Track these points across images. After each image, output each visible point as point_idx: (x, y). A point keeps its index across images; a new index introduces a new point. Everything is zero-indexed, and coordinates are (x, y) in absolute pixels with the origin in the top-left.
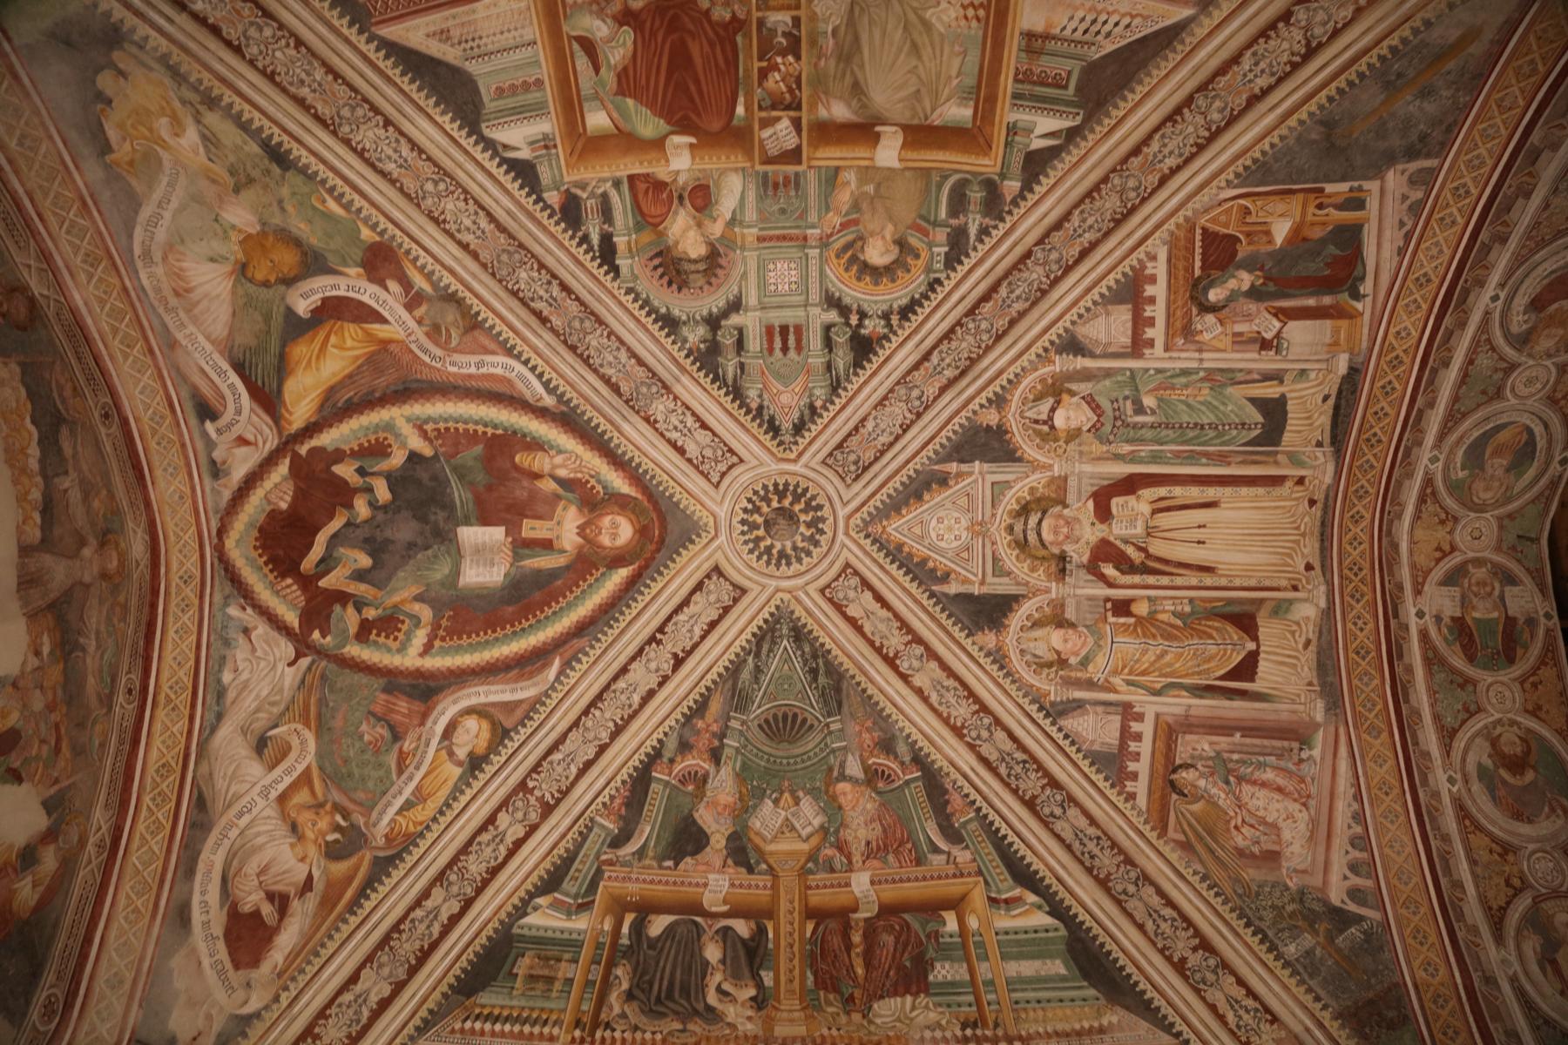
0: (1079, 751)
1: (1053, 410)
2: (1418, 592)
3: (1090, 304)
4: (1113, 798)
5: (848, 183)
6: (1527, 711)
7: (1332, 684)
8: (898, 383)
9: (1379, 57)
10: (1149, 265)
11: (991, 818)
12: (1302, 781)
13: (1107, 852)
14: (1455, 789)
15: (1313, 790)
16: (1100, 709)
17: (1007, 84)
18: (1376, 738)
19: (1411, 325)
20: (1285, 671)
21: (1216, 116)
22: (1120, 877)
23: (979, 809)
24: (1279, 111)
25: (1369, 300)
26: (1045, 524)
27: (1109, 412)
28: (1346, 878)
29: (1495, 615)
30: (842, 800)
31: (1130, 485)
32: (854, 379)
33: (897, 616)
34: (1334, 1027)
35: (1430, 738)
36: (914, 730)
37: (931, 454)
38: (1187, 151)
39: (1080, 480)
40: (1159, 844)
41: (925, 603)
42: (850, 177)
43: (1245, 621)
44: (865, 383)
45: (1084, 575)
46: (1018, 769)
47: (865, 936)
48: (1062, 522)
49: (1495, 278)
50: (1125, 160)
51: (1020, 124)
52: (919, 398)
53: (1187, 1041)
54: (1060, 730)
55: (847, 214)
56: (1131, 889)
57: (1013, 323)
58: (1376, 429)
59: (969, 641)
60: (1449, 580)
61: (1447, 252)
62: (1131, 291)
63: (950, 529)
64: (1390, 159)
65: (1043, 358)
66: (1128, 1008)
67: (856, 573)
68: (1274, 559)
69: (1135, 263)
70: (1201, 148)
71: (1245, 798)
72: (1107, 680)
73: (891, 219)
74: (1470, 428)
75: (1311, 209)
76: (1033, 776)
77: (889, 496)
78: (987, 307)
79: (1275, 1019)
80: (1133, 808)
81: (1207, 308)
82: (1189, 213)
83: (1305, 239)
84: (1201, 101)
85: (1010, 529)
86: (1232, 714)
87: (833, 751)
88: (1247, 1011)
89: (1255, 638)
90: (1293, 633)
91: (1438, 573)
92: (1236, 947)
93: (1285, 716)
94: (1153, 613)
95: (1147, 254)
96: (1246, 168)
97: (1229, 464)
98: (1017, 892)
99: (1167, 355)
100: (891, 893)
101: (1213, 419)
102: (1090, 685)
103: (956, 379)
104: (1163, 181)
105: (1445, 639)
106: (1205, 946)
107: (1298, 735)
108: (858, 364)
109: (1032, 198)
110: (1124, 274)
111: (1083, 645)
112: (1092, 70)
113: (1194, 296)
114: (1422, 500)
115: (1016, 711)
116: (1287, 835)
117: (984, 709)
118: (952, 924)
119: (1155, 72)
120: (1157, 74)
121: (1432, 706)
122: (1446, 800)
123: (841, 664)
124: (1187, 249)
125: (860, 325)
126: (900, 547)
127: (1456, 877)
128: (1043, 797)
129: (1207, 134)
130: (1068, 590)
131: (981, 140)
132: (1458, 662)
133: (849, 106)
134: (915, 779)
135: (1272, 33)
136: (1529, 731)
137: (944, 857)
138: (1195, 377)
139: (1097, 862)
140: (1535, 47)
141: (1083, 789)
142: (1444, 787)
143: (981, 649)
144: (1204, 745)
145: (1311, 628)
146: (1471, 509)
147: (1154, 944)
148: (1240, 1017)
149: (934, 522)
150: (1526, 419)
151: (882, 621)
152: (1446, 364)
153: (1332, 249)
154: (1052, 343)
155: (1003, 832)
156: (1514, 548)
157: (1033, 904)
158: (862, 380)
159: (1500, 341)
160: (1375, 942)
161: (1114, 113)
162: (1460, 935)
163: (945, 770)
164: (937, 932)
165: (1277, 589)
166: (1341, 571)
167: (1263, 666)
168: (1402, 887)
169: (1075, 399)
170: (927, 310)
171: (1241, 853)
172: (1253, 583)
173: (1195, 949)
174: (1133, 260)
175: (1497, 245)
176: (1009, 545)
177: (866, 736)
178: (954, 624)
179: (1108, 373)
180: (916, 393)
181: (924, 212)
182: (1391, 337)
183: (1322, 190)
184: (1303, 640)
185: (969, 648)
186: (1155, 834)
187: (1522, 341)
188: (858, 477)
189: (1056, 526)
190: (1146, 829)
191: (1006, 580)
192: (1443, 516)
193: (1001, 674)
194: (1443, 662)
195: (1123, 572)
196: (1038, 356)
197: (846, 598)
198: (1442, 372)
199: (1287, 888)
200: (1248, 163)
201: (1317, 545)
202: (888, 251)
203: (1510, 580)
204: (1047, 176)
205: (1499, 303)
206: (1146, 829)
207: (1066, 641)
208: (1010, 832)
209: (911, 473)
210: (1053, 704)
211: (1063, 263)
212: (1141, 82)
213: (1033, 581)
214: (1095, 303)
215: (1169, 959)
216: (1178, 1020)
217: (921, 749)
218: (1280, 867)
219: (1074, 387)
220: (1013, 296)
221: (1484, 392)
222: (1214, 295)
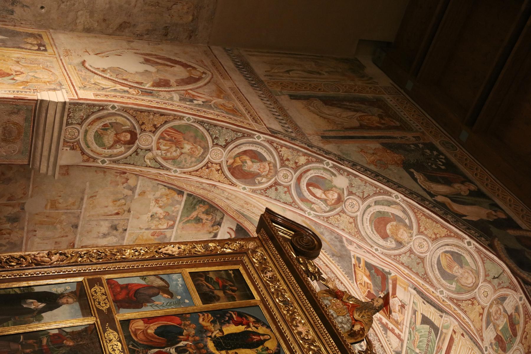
25: (391, 271)
74: (434, 274)
138: (412, 332)
146: (473, 290)
150: (440, 252)
159: (397, 252)
183: (354, 265)
187: (400, 244)
203: (502, 299)
205: (379, 249)
221: (418, 264)
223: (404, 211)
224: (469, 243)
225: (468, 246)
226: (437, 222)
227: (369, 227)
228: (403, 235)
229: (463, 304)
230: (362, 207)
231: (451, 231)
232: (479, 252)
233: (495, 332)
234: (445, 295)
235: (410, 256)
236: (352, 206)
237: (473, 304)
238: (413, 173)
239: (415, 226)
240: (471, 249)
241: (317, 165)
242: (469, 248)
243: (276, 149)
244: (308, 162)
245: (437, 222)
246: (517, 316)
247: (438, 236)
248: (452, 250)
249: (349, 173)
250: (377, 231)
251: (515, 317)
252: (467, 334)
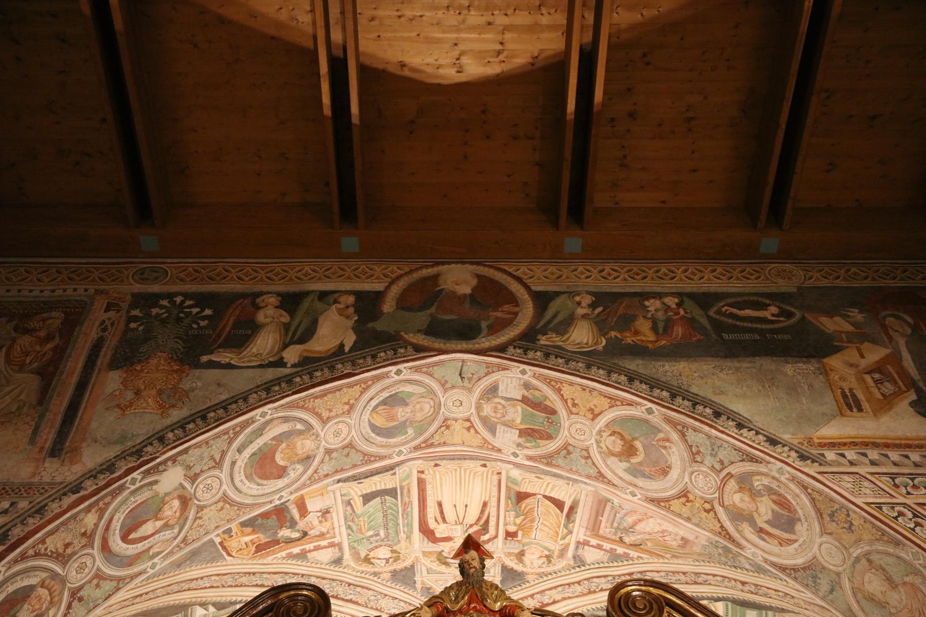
2: (499, 450)
6: (593, 419)
29: (519, 408)
60: (493, 430)
86: (586, 516)
105: (535, 447)
136: (607, 426)
146: (439, 413)
159: (310, 472)
165: (500, 481)
172: (495, 489)
183: (221, 543)
184: (536, 479)
201: (468, 461)
203: (493, 390)
223: (286, 419)
225: (400, 376)
226: (339, 389)
227: (251, 486)
228: (305, 445)
229: (437, 439)
230: (224, 475)
231: (365, 381)
232: (417, 369)
233: (514, 431)
235: (331, 459)
236: (209, 488)
237: (448, 427)
238: (210, 361)
239: (314, 421)
241: (119, 499)
242: (401, 377)
243: (37, 555)
244: (102, 512)
245: (339, 389)
246: (537, 393)
247: (351, 402)
248: (381, 399)
249: (173, 459)
250: (267, 478)
251: (534, 396)
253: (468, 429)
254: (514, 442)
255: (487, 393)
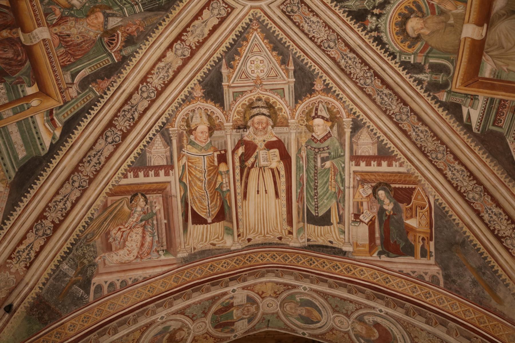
0: (145, 146)
1: (323, 118)
2: (243, 288)
3: (378, 135)
4: (122, 167)
5: (457, 8)
6: (194, 337)
7: (196, 258)
8: (338, 35)
9: (498, 270)
10: (397, 163)
11: (99, 104)
12: (148, 254)
13: (93, 169)
14: (158, 320)
15: (145, 260)
16: (168, 154)
17: (499, 95)
18: (174, 281)
19: (367, 276)
20: (199, 237)
21: (471, 196)
22: (82, 176)
23: (102, 97)
24: (471, 223)
25: (378, 259)
26: (263, 117)
27: (322, 145)
28: (106, 282)
29: (235, 318)
30: (93, 17)
31: (285, 157)
32: (342, 11)
33: (205, 40)
34: (33, 294)
35: (179, 304)
36: (141, 55)
37: (298, 54)
38: (455, 182)
39: (287, 133)
40: (103, 194)
41: (215, 56)
42: (460, 9)
43: (222, 215)
44: (339, 17)
45: (237, 138)
46: (129, 116)
47: (8, 39)
48: (264, 125)
49: (390, 311)
50: (452, 152)
51: (477, 101)
52: (329, 46)
53: (2, 229)
54: (154, 135)
55: (438, 6)
56: (76, 184)
57: (369, 96)
58: (316, 263)
59: (196, 82)
60: (250, 299)
61: (400, 290)
62: (384, 155)
63: (257, 67)
64: (445, 268)
65: (350, 112)
66: (10, 195)
67: (229, 14)
68: (252, 225)
69: (399, 157)
70: (455, 188)
71: (135, 230)
72: (184, 155)
73: (433, 32)
74: (319, 301)
75: (422, 236)
76: (127, 124)
77: (274, 32)
78: (378, 83)
79: (28, 268)
80: (119, 178)
81: (375, 190)
82: (423, 182)
83: (408, 233)
84: (479, 189)
85: (259, 99)
87: (122, 9)
88: (28, 254)
89: (213, 222)
90: (218, 238)
91: (252, 294)
92: (59, 241)
93: (178, 240)
94: (221, 173)
95: (403, 162)
96: (444, 208)
97: (298, 202)
98: (59, 125)
99: (352, 172)
100: (41, 53)
101: (320, 194)
102: (180, 148)
103: (339, 66)
104: (440, 170)
105: (223, 302)
106: (56, 227)
107: (170, 247)
108: (350, 13)
109: (436, 107)
110: (393, 151)
111: (201, 142)
112: (501, 138)
113: (381, 184)
114: (285, 285)
115: (160, 111)
116: (121, 252)
117: (159, 94)
118: (31, 90)
119: (496, 168)
120: (495, 170)
121: (194, 303)
122: (153, 318)
123: (175, 9)
124: (405, 181)
125: (373, 15)
126: (246, 40)
127: (119, 329)
128: (116, 131)
129: (462, 191)
130: (229, 131)
131: (470, 82)
132: (214, 309)
133: (501, 9)
134: (113, 59)
135: (510, 222)
137: (70, 81)
138: (340, 185)
139: (86, 164)
140: (491, 324)
141: (125, 151)
142: (158, 316)
143: (192, 89)
144: (159, 207)
145: (221, 245)
146: (281, 303)
147: (50, 201)
148: (24, 251)
149: (260, 58)
150: (323, 321)
151: (202, 31)
152: (349, 292)
153: (402, 244)
154: (358, 116)
155: (92, 112)
156: (264, 319)
157: (54, 134)
158: (341, 15)
159: (361, 312)
160: (79, 302)
161: (477, 148)
162: (92, 336)
163: (121, 76)
164: (24, 83)
166: (249, 253)
167: (200, 227)
168: (107, 307)
169: (329, 129)
170: (379, 52)
171: (108, 233)
172: (240, 217)
173: (53, 222)
174: (400, 155)
175: (404, 311)
176: (250, 99)
177: (134, 28)
178: (205, 73)
179: (342, 145)
180: (332, 44)
181: (434, 50)
182: (361, 268)
183: (431, 240)
184: (215, 242)
185: (192, 82)
186: (108, 191)
187: (360, 320)
188: (284, 12)
189: (262, 123)
190: (110, 186)
191: (232, 99)
192: (278, 293)
193: (180, 100)
194: (213, 303)
195: (240, 158)
196: (352, 109)
197: (213, 8)
198: (345, 290)
199: (95, 258)
200: (446, 209)
201: (260, 242)
202: (414, 31)
203: (250, 320)
204: (447, 114)
205: (379, 312)
206: (110, 186)
207: (202, 133)
208: (93, 116)
209: (288, 44)
210: (167, 130)
211: (400, 121)
212: (492, 161)
213: (232, 113)
214: (379, 137)
215: (44, 210)
216: (12, 222)
217: (131, 61)
218: (104, 252)
219: (335, 128)
220: (384, 96)
221: (337, 306)
222: (381, 193)
224: (304, 334)
227: (396, 333)
231: (322, 339)
232: (294, 331)
233: (237, 304)
234: (301, 288)
235: (347, 311)
240: (301, 331)
242: (302, 331)
247: (331, 333)
248: (314, 325)
250: (386, 329)
251: (228, 328)
252: (276, 244)
253: (263, 293)
254: (236, 298)
255: (253, 318)
